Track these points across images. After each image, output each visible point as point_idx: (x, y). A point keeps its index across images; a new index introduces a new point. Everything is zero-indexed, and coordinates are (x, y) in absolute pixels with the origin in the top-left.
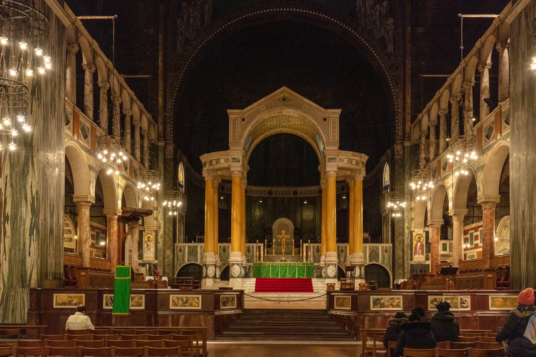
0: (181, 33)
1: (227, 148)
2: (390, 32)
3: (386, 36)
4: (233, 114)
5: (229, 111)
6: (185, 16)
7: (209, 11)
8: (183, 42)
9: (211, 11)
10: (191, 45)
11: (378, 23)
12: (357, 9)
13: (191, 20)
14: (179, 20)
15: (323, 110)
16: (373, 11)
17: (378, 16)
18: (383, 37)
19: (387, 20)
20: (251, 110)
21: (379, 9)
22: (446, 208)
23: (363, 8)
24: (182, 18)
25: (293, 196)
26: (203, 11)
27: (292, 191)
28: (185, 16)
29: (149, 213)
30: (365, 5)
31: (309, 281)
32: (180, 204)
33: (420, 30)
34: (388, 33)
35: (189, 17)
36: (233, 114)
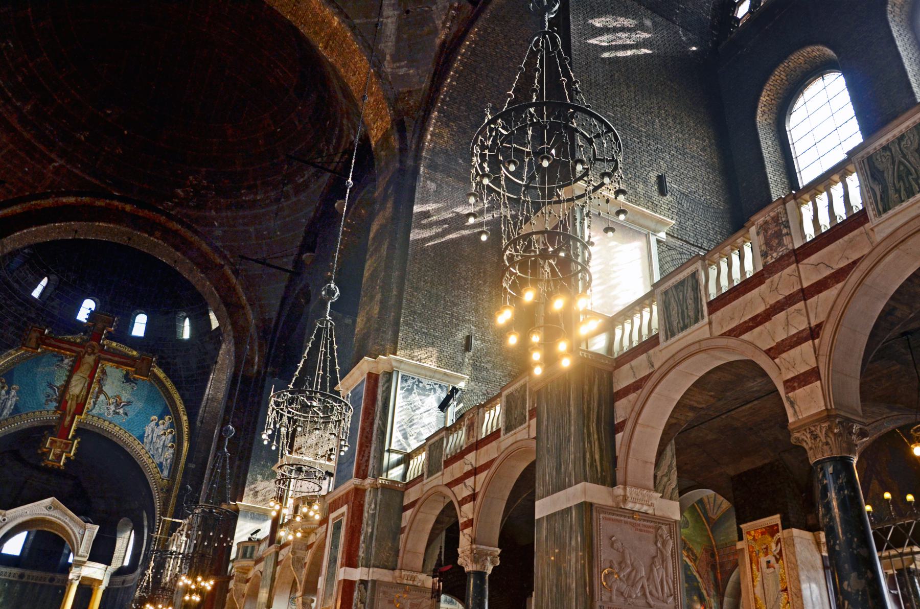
3: (164, 463)
7: (11, 406)
9: (12, 407)
11: (160, 450)
12: (146, 435)
18: (161, 463)
19: (168, 450)
20: (15, 512)
21: (163, 440)
23: (150, 436)
25: (47, 583)
27: (49, 577)
30: (153, 433)
33: (192, 466)
34: (166, 460)
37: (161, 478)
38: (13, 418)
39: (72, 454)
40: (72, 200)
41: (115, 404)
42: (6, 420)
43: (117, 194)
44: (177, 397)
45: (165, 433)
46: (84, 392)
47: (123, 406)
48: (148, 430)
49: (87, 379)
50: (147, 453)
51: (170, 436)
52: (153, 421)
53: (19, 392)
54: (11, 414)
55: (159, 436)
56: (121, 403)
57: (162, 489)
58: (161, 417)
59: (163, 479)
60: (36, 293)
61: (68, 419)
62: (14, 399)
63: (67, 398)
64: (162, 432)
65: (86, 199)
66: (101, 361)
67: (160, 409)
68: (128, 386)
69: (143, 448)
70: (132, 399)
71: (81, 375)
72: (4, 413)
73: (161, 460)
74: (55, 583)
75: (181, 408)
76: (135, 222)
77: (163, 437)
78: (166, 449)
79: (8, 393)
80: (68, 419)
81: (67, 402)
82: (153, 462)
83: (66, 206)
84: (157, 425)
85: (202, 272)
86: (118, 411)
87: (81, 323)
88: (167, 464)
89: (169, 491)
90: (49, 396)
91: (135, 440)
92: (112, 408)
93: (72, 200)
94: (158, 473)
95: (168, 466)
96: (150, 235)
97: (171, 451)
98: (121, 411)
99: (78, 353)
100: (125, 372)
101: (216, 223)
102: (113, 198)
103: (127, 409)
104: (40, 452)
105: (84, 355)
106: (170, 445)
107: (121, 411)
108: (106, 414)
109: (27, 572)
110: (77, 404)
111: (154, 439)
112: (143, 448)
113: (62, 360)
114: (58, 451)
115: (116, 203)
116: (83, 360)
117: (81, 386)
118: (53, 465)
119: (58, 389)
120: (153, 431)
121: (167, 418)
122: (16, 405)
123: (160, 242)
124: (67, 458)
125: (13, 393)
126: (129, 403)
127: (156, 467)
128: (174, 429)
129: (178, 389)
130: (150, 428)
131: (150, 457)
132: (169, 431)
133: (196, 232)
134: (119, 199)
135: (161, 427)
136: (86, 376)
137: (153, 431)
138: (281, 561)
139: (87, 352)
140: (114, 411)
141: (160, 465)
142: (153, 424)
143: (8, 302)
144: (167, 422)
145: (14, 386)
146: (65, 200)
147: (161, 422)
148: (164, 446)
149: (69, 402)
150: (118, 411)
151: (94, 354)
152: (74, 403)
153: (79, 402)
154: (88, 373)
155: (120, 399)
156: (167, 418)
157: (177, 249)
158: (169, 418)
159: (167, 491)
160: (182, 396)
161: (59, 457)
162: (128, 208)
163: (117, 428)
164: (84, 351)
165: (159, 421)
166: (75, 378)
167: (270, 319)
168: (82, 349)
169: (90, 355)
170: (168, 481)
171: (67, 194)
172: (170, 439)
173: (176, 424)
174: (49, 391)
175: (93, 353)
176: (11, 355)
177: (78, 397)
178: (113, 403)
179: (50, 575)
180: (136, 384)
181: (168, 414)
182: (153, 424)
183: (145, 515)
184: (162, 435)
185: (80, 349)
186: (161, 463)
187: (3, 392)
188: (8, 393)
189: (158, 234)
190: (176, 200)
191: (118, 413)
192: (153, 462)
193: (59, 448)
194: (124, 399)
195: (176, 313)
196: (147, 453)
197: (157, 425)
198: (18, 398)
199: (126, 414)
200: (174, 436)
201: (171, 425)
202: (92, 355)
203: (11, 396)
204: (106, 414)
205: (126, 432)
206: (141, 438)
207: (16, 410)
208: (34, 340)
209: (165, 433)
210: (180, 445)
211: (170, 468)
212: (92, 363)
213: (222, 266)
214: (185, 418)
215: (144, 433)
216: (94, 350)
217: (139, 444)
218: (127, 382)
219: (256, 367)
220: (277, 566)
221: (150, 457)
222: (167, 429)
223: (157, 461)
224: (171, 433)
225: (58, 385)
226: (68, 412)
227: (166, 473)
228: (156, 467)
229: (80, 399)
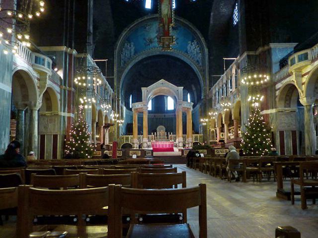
1: (142, 101)
4: (144, 89)
5: (142, 88)
15: (176, 87)
22: (222, 121)
28: (124, 54)
29: (113, 125)
31: (173, 149)
32: (123, 121)
35: (125, 54)
36: (144, 89)
46: (169, 12)
48: (188, 48)
53: (134, 45)
55: (194, 49)
58: (192, 41)
61: (166, 26)
63: (162, 17)
72: (132, 54)
74: (166, 117)
75: (199, 35)
79: (130, 46)
80: (166, 26)
84: (192, 45)
88: (200, 60)
89: (204, 71)
97: (200, 54)
109: (156, 115)
110: (168, 19)
113: (145, 28)
114: (167, 43)
117: (167, 9)
120: (190, 48)
121: (195, 41)
122: (135, 50)
125: (132, 46)
135: (193, 45)
142: (190, 45)
148: (197, 53)
149: (164, 19)
152: (166, 18)
156: (195, 41)
163: (176, 50)
173: (199, 43)
174: (145, 41)
177: (167, 15)
179: (164, 114)
182: (190, 45)
183: (193, 86)
188: (130, 46)
197: (192, 45)
199: (177, 43)
201: (198, 44)
206: (187, 52)
207: (136, 52)
214: (203, 38)
227: (201, 64)
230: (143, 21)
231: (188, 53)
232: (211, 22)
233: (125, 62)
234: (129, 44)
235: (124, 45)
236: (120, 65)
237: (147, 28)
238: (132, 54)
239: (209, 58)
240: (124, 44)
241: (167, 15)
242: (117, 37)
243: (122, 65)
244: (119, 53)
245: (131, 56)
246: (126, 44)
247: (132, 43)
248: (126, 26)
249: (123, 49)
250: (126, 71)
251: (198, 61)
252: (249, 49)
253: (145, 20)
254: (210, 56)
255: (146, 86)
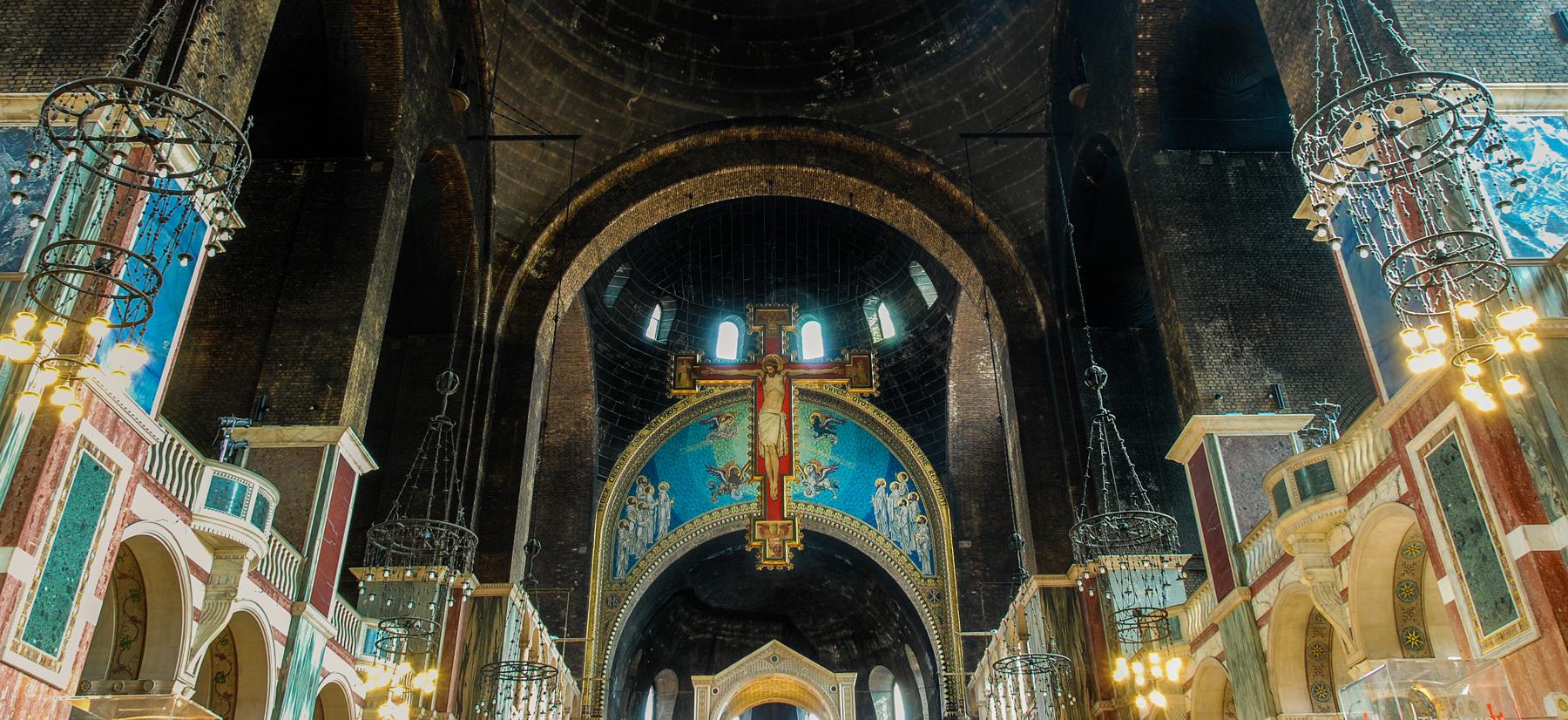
0: (625, 549)
2: (924, 545)
3: (919, 551)
6: (632, 527)
8: (626, 562)
9: (669, 517)
10: (638, 566)
11: (906, 532)
13: (640, 529)
14: (622, 531)
16: (897, 516)
17: (905, 522)
18: (915, 553)
20: (726, 676)
21: (906, 513)
23: (884, 513)
24: (627, 528)
26: (657, 518)
28: (632, 527)
30: (886, 507)
33: (966, 544)
34: (921, 546)
35: (637, 526)
37: (921, 578)
38: (675, 533)
39: (798, 542)
40: (671, 147)
41: (813, 475)
42: (667, 538)
43: (732, 117)
44: (903, 437)
45: (904, 501)
47: (827, 473)
48: (877, 502)
49: (782, 414)
50: (886, 541)
51: (914, 504)
52: (879, 486)
53: (671, 492)
54: (670, 529)
56: (822, 471)
57: (930, 596)
58: (890, 478)
59: (926, 580)
60: (651, 333)
61: (774, 485)
62: (668, 505)
63: (762, 453)
64: (900, 502)
65: (690, 141)
66: (794, 382)
67: (884, 464)
68: (825, 441)
69: (878, 535)
70: (837, 460)
71: (770, 410)
73: (914, 548)
75: (917, 454)
76: (769, 152)
77: (904, 508)
78: (915, 527)
79: (656, 496)
80: (774, 485)
81: (764, 459)
82: (901, 554)
83: (665, 160)
84: (888, 491)
85: (899, 196)
86: (821, 484)
87: (726, 365)
88: (923, 552)
89: (941, 596)
90: (714, 487)
91: (861, 524)
92: (811, 481)
93: (671, 147)
94: (915, 570)
95: (928, 554)
96: (802, 164)
97: (924, 528)
98: (826, 483)
99: (755, 378)
100: (812, 420)
101: (896, 111)
102: (727, 124)
103: (834, 477)
104: (749, 549)
105: (764, 378)
106: (918, 519)
107: (826, 483)
108: (805, 494)
111: (891, 516)
112: (878, 535)
113: (716, 426)
115: (735, 132)
116: (764, 387)
118: (775, 566)
119: (724, 473)
120: (885, 503)
121: (899, 476)
122: (673, 513)
123: (819, 170)
124: (793, 550)
125: (663, 495)
126: (834, 468)
127: (908, 562)
128: (916, 491)
129: (903, 424)
130: (878, 499)
131: (894, 548)
132: (909, 496)
133: (868, 136)
134: (741, 122)
135: (895, 493)
136: (778, 411)
137: (885, 503)
138: (1266, 616)
139: (767, 372)
140: (816, 486)
141: (914, 556)
143: (618, 356)
144: (903, 484)
145: (661, 484)
146: (661, 151)
147: (892, 485)
149: (767, 459)
150: (821, 484)
151: (779, 373)
153: (781, 454)
154: (780, 405)
155: (819, 465)
156: (899, 476)
157: (848, 174)
158: (903, 475)
159: (938, 596)
160: (912, 434)
161: (779, 551)
162: (755, 132)
164: (762, 373)
165: (888, 484)
166: (763, 417)
167: (1042, 233)
168: (758, 371)
169: (772, 376)
170: (935, 579)
171: (663, 140)
172: (915, 509)
173: (916, 484)
174: (712, 479)
175: (777, 372)
176: (644, 437)
178: (810, 474)
180: (833, 434)
181: (900, 469)
182: (882, 488)
183: (910, 653)
184: (901, 505)
185: (755, 371)
186: (915, 553)
187: (650, 497)
188: (656, 496)
189: (811, 159)
190: (823, 96)
191: (821, 488)
192: (901, 554)
193: (776, 535)
194: (824, 463)
195: (861, 302)
196: (886, 541)
197: (888, 491)
198: (672, 502)
200: (920, 503)
201: (911, 487)
202: (776, 375)
203: (662, 500)
204: (805, 494)
205: (843, 516)
206: (870, 519)
207: (676, 521)
208: (684, 376)
209: (904, 501)
210: (934, 515)
211: (931, 558)
212: (781, 388)
213: (929, 175)
214: (929, 468)
215: (873, 508)
216: (776, 368)
217: (870, 529)
218: (820, 434)
219: (1043, 320)
220: (1259, 628)
221: (894, 548)
222: (906, 494)
223: (907, 550)
224: (914, 498)
225: (722, 466)
226: (770, 475)
227: (927, 567)
228: (908, 562)
229: (782, 449)
230: (707, 402)
231: (876, 526)
232: (953, 411)
233: (632, 560)
234: (652, 490)
235: (633, 492)
236: (615, 575)
237: (722, 426)
238: (663, 526)
239: (956, 546)
240: (634, 487)
241: (776, 447)
242: (607, 465)
243: (621, 574)
244: (612, 522)
245: (655, 535)
246: (640, 489)
247: (664, 484)
248: (641, 427)
249: (630, 508)
250: (636, 595)
251: (914, 556)
252: (1044, 568)
253: (715, 399)
254: (958, 536)
255: (711, 669)
